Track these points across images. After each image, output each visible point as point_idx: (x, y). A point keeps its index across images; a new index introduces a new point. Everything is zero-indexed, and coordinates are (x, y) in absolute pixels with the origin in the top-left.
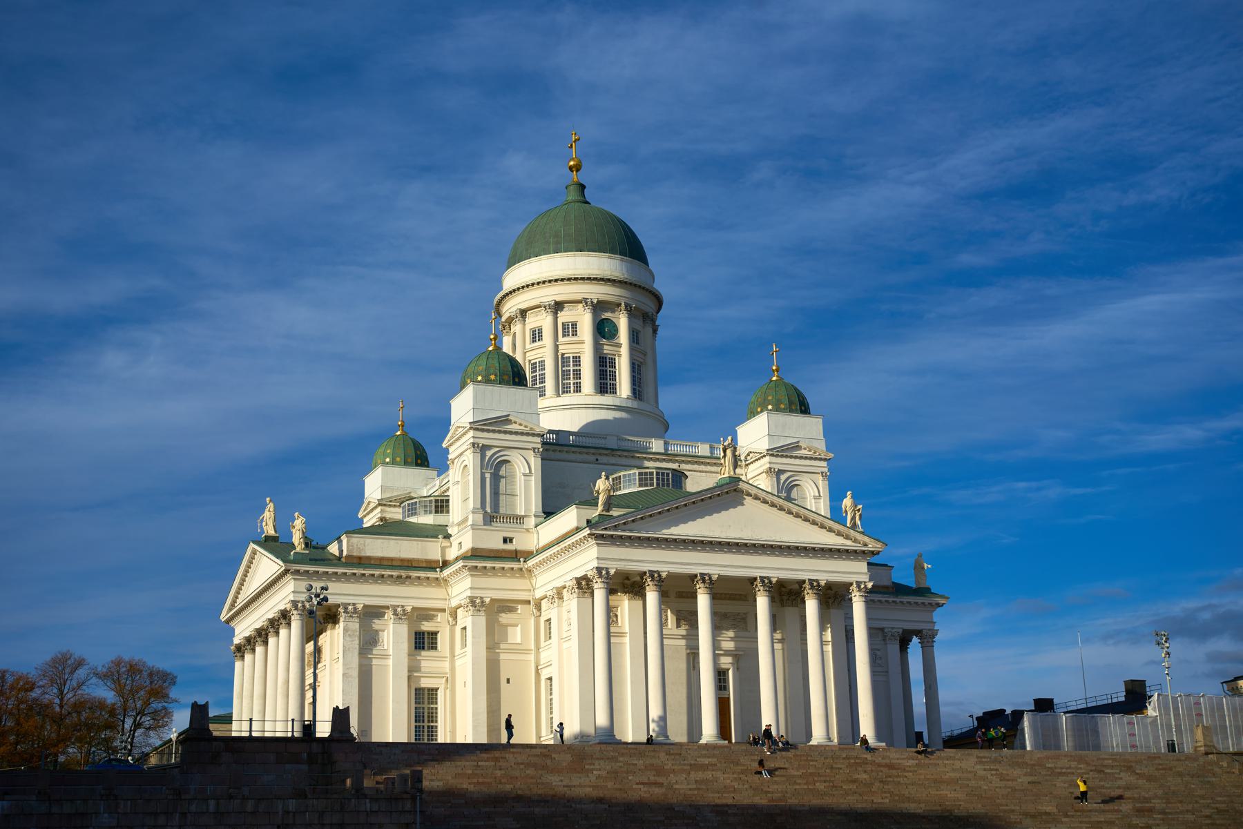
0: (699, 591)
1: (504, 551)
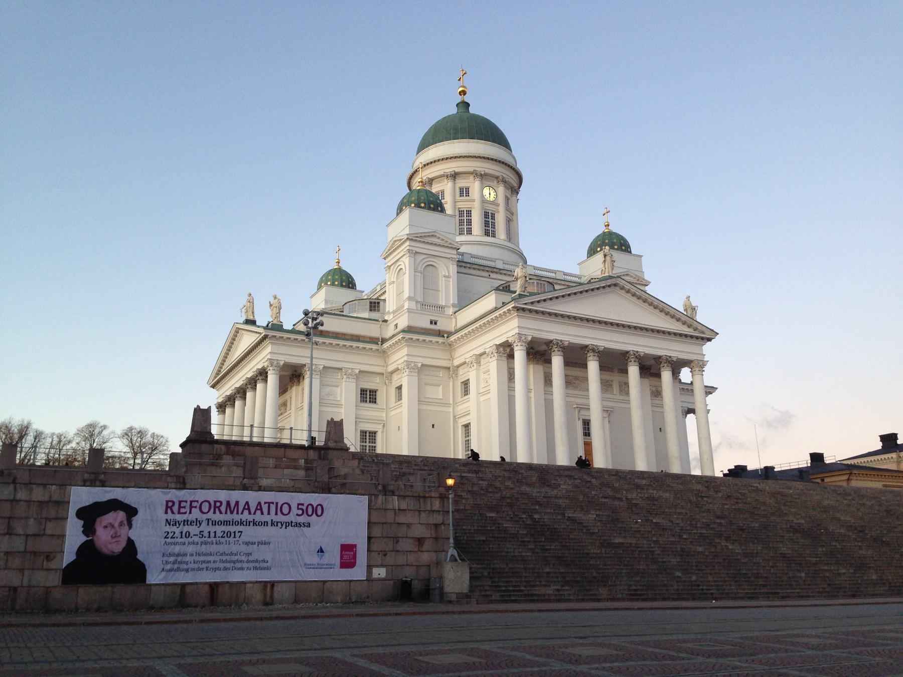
0: (589, 358)
1: (433, 330)
